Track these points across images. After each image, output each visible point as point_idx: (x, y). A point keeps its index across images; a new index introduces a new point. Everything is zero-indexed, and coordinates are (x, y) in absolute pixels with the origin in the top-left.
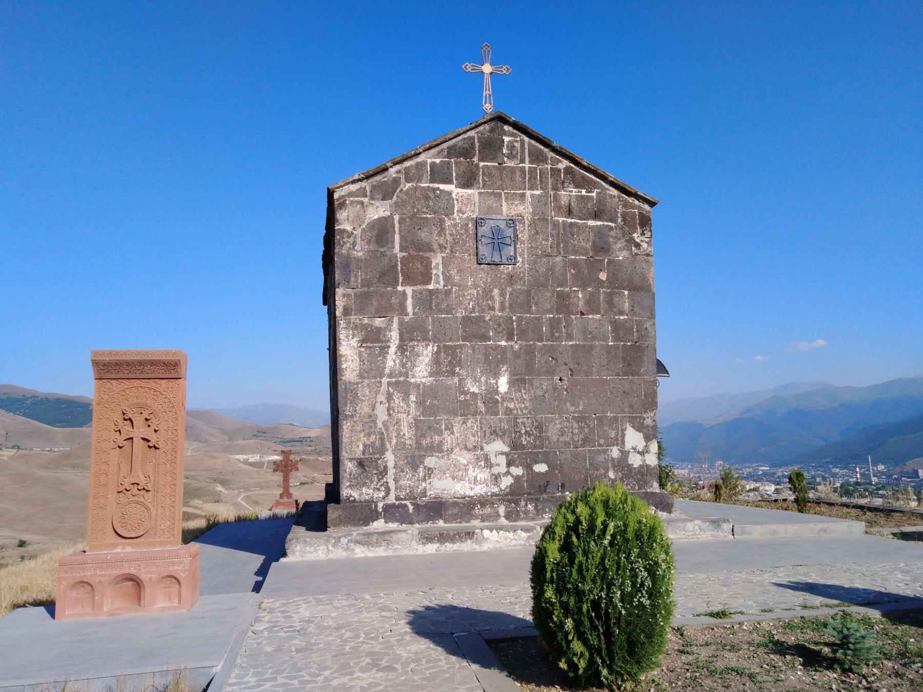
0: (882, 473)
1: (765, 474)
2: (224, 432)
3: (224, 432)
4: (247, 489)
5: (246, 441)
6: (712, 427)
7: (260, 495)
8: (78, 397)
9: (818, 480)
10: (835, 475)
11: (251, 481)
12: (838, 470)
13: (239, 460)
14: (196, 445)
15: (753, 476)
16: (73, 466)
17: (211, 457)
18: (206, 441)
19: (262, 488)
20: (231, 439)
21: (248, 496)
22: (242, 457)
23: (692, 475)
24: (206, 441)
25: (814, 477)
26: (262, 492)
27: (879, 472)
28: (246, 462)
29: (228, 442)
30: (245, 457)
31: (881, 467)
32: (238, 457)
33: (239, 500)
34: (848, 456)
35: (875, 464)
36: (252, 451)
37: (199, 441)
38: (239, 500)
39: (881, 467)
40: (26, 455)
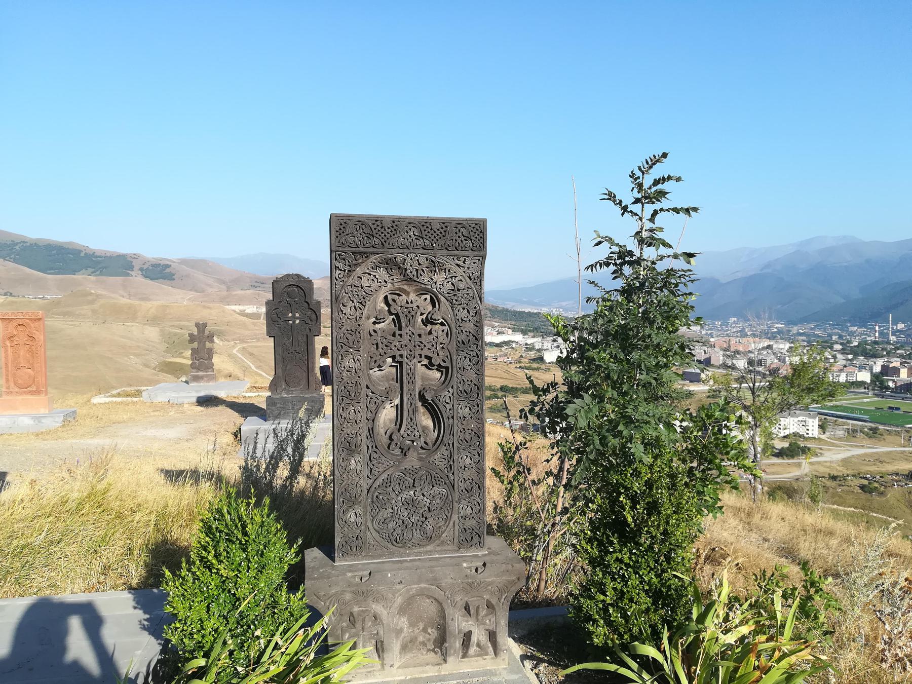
0: (900, 331)
1: (780, 331)
2: (223, 282)
3: (223, 282)
4: (242, 341)
5: (243, 292)
6: (729, 283)
7: (256, 347)
8: (70, 243)
9: (834, 338)
10: (852, 334)
11: (247, 332)
12: (856, 328)
13: (234, 311)
14: (192, 294)
15: (767, 333)
16: (65, 314)
17: (204, 307)
18: (203, 291)
19: (258, 340)
20: (228, 289)
21: (244, 348)
22: (237, 308)
23: (703, 332)
24: (203, 291)
25: (830, 335)
26: (259, 344)
27: (898, 331)
28: (242, 313)
29: (225, 293)
30: (242, 308)
31: (901, 326)
32: (233, 307)
33: (235, 351)
34: (868, 315)
35: (895, 323)
36: (250, 302)
37: (196, 291)
38: (235, 351)
39: (901, 326)
40: (16, 302)
